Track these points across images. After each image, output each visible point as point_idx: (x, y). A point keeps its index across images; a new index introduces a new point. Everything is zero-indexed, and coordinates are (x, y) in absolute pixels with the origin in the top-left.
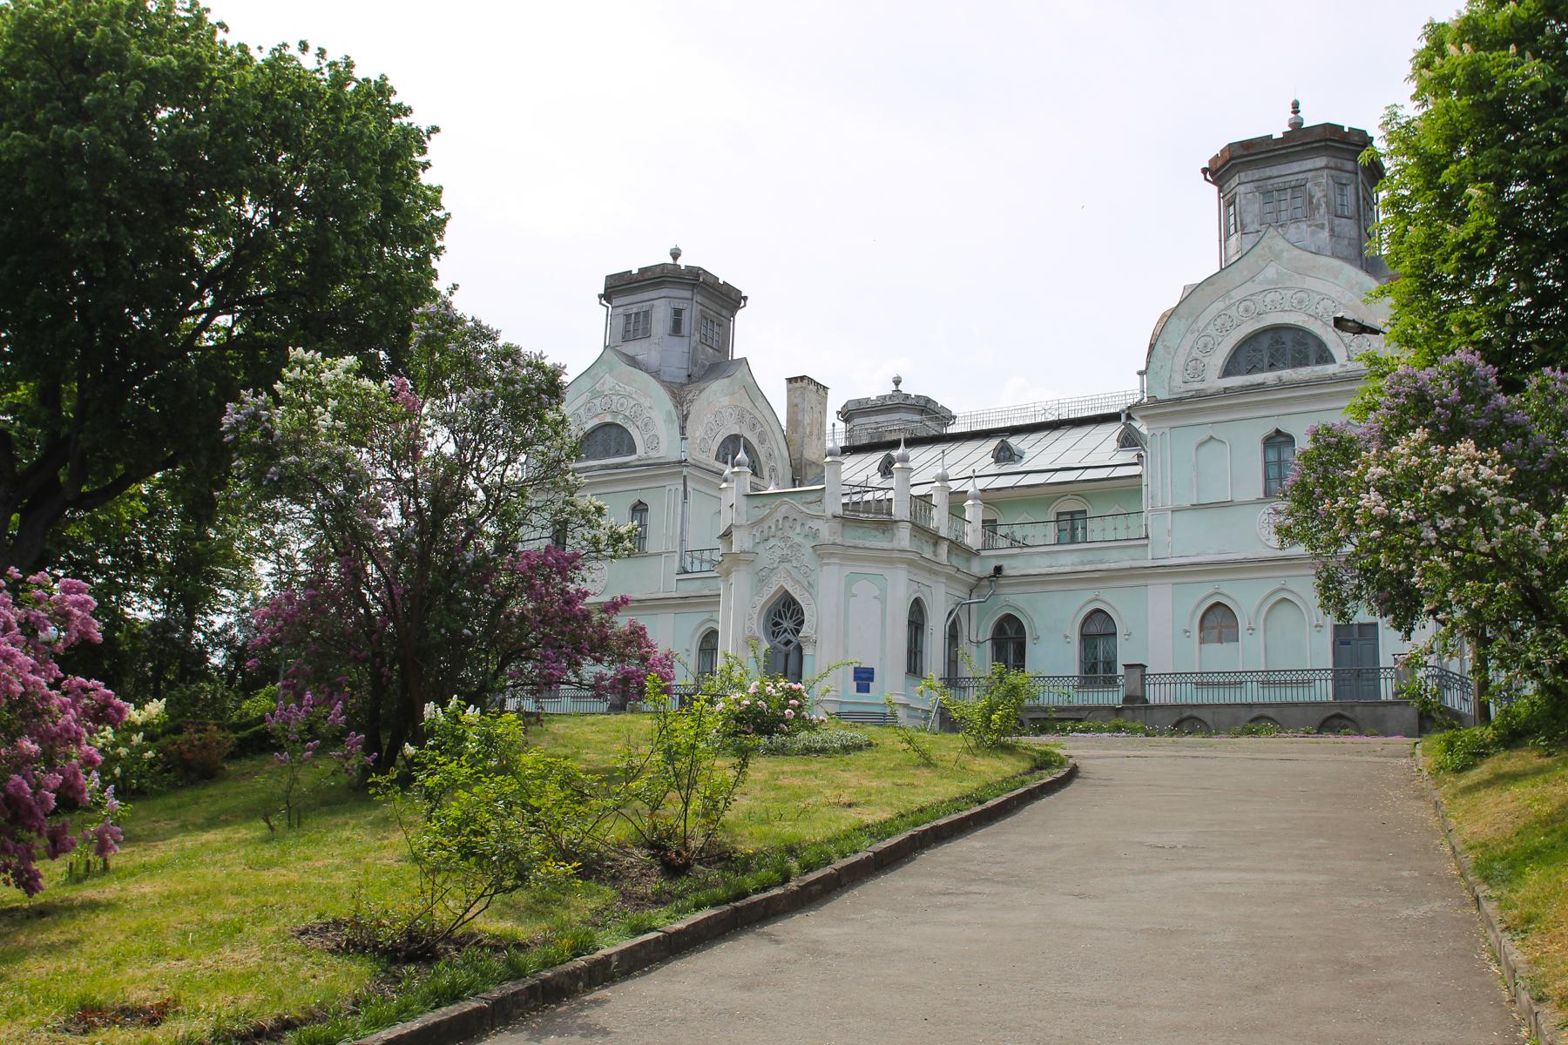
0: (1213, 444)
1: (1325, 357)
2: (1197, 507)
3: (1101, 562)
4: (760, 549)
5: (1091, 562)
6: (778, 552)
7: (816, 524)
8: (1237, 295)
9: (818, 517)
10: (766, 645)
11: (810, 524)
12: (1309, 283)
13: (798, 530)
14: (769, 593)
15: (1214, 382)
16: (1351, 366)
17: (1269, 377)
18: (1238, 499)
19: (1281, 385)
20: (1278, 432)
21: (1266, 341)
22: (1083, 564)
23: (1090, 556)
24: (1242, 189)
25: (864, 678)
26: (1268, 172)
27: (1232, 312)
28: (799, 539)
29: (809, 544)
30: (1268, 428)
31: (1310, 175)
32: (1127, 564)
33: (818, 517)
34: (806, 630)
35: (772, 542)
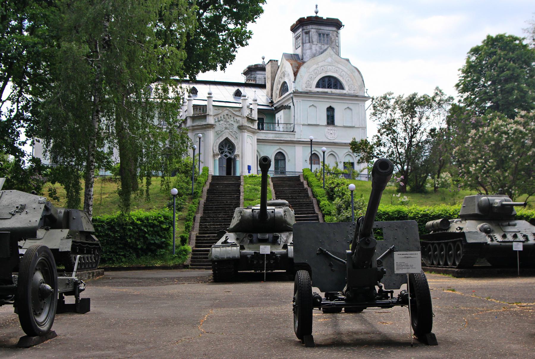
0: (312, 107)
1: (342, 88)
2: (309, 125)
3: (281, 137)
4: (217, 124)
5: (278, 137)
6: (225, 126)
7: (238, 118)
8: (320, 64)
9: (239, 116)
10: (220, 156)
11: (236, 118)
12: (339, 66)
13: (232, 119)
14: (222, 139)
15: (314, 89)
16: (349, 92)
17: (329, 90)
18: (320, 124)
19: (332, 94)
20: (330, 106)
21: (327, 80)
22: (275, 137)
23: (278, 135)
24: (313, 30)
25: (249, 168)
26: (322, 28)
27: (319, 69)
28: (232, 123)
29: (236, 125)
30: (328, 106)
31: (331, 32)
32: (289, 139)
33: (239, 116)
34: (236, 153)
35: (221, 122)
